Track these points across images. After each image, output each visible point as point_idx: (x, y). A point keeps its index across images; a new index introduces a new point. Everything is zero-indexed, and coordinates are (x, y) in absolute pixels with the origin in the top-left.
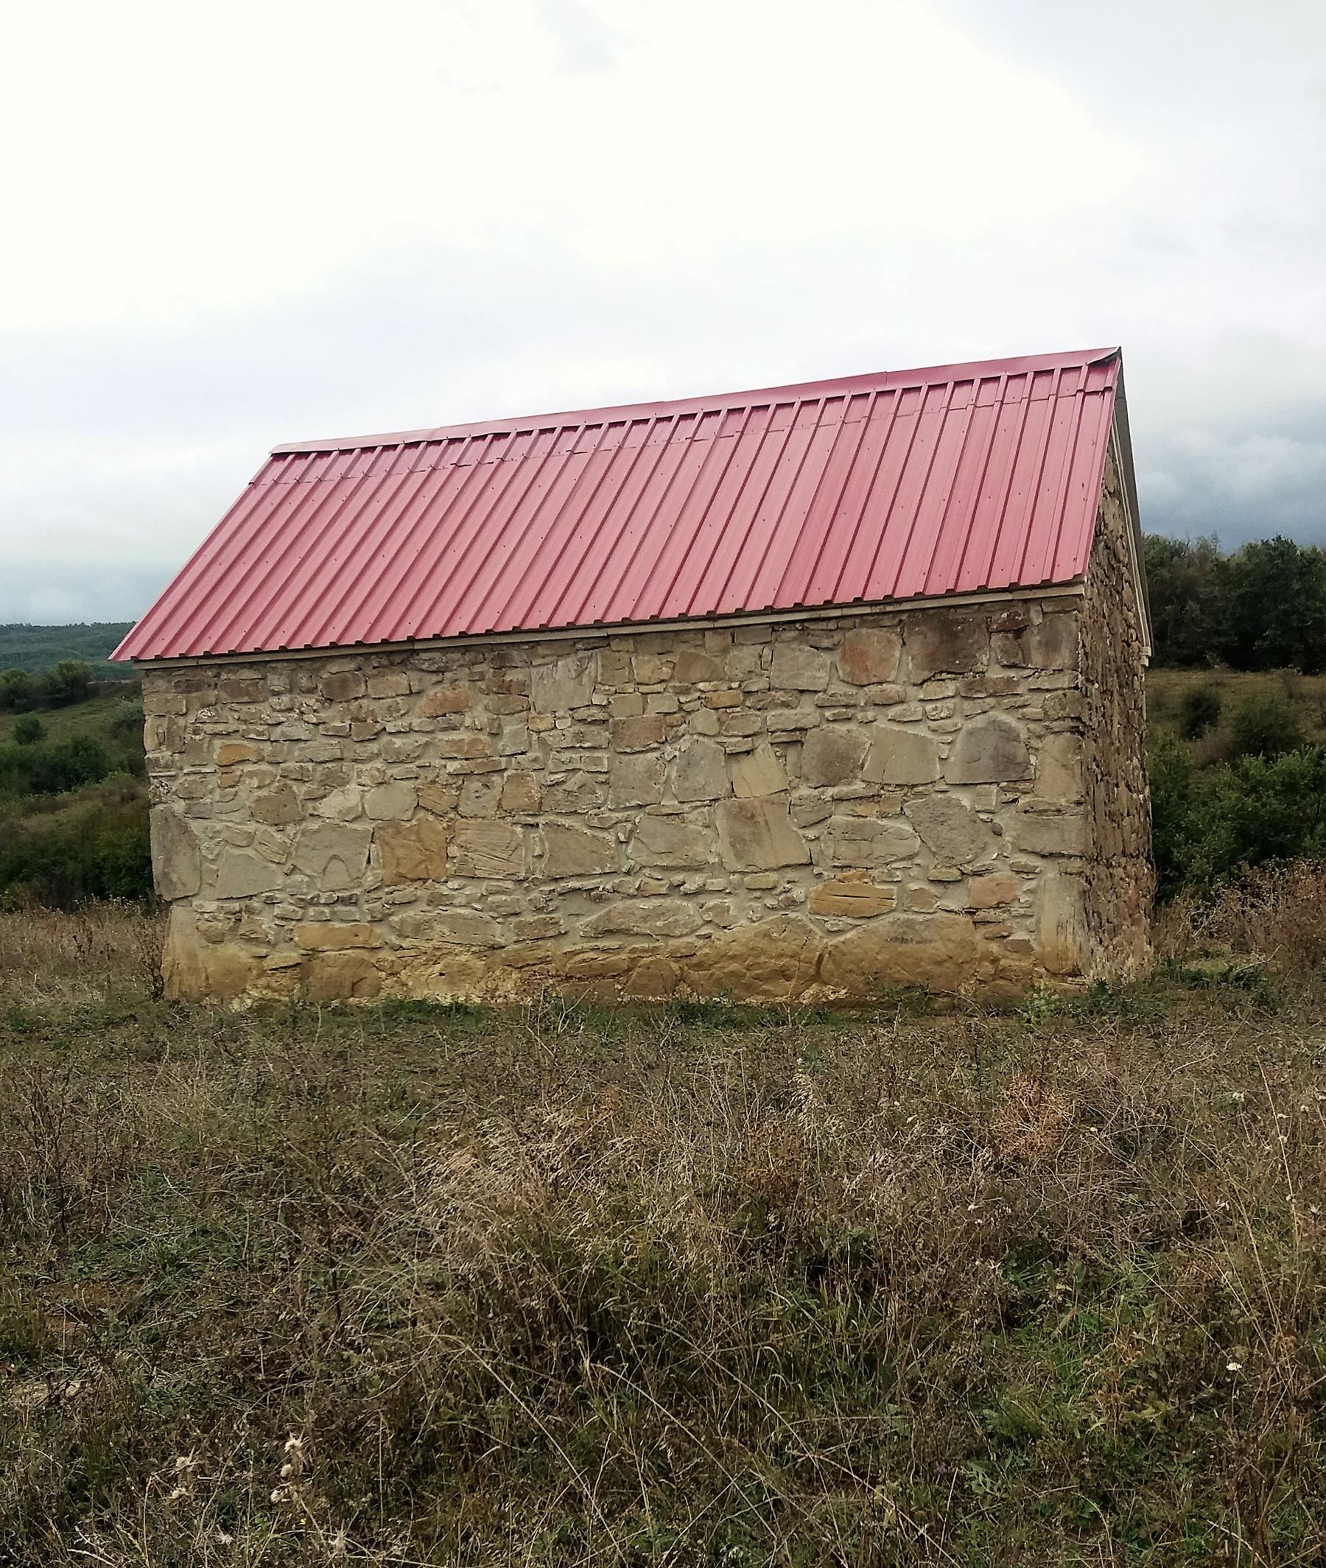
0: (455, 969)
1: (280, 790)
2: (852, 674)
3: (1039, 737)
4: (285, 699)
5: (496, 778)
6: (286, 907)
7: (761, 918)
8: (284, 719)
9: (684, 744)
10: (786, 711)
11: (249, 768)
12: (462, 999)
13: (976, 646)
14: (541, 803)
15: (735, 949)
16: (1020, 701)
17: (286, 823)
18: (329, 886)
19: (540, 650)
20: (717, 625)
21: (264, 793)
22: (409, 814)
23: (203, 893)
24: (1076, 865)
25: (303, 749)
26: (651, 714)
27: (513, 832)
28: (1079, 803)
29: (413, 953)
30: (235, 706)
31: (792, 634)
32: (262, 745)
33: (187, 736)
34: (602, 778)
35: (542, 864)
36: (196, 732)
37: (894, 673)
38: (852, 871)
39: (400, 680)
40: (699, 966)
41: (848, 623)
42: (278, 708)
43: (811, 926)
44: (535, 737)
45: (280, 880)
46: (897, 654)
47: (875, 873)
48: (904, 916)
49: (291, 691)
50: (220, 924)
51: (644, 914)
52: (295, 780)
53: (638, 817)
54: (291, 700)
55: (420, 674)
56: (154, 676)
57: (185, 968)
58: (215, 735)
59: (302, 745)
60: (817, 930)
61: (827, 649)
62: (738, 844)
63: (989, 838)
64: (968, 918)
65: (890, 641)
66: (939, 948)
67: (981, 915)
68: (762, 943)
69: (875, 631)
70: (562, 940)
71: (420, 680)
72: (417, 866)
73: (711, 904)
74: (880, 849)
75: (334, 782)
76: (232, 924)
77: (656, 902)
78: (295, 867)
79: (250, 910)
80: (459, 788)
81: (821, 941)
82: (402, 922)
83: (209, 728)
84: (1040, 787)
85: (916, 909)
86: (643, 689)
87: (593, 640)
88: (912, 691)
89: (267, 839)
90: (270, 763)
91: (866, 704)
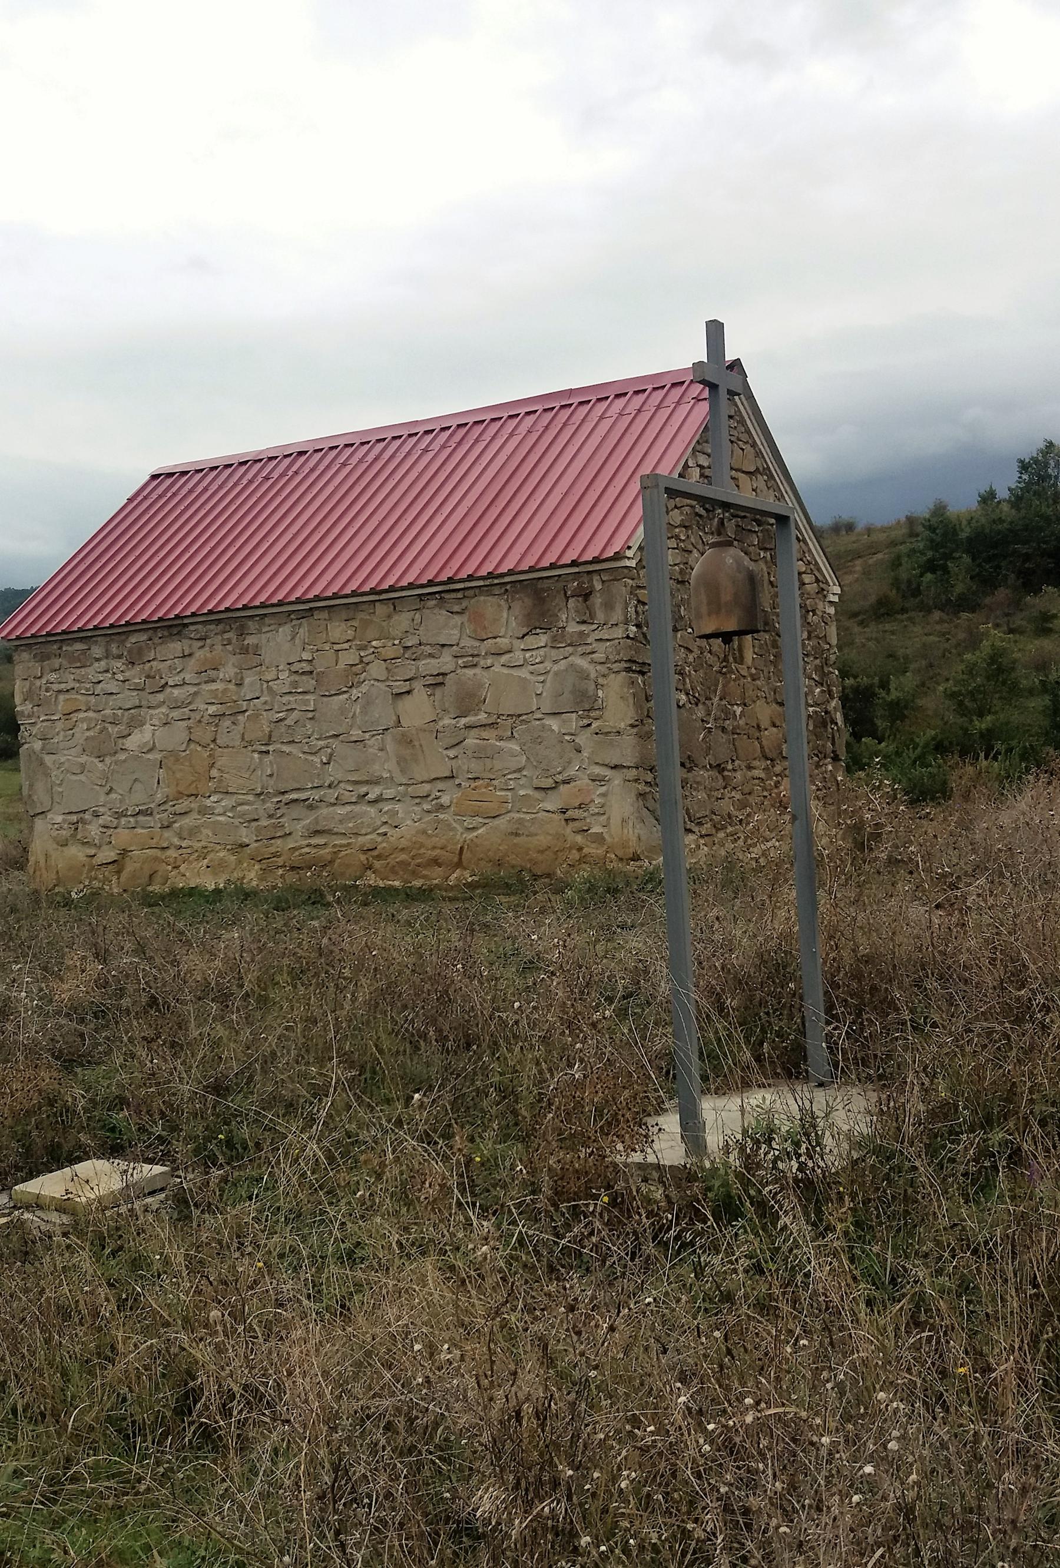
1: (101, 732)
2: (475, 631)
3: (604, 676)
4: (103, 663)
5: (240, 717)
6: (106, 819)
7: (420, 819)
9: (364, 688)
10: (432, 661)
11: (82, 715)
14: (270, 736)
15: (404, 843)
16: (589, 649)
17: (105, 755)
19: (267, 620)
21: (91, 733)
22: (184, 745)
24: (632, 773)
26: (341, 665)
27: (252, 758)
28: (632, 726)
29: (189, 851)
31: (434, 602)
34: (310, 715)
35: (271, 782)
37: (503, 630)
38: (481, 782)
39: (176, 647)
40: (379, 857)
43: (455, 825)
45: (102, 799)
46: (505, 615)
48: (517, 816)
49: (107, 658)
50: (64, 832)
53: (335, 743)
54: (107, 664)
55: (190, 642)
58: (60, 691)
60: (458, 827)
61: (457, 613)
62: (401, 761)
63: (573, 754)
64: (562, 816)
65: (499, 606)
66: (543, 840)
67: (569, 813)
68: (422, 839)
69: (489, 598)
70: (289, 839)
71: (190, 646)
73: (386, 809)
74: (498, 764)
75: (135, 724)
77: (348, 808)
78: (111, 789)
80: (217, 725)
81: (462, 837)
82: (181, 827)
83: (55, 687)
84: (607, 714)
85: (524, 810)
86: (336, 647)
88: (516, 642)
91: (486, 654)
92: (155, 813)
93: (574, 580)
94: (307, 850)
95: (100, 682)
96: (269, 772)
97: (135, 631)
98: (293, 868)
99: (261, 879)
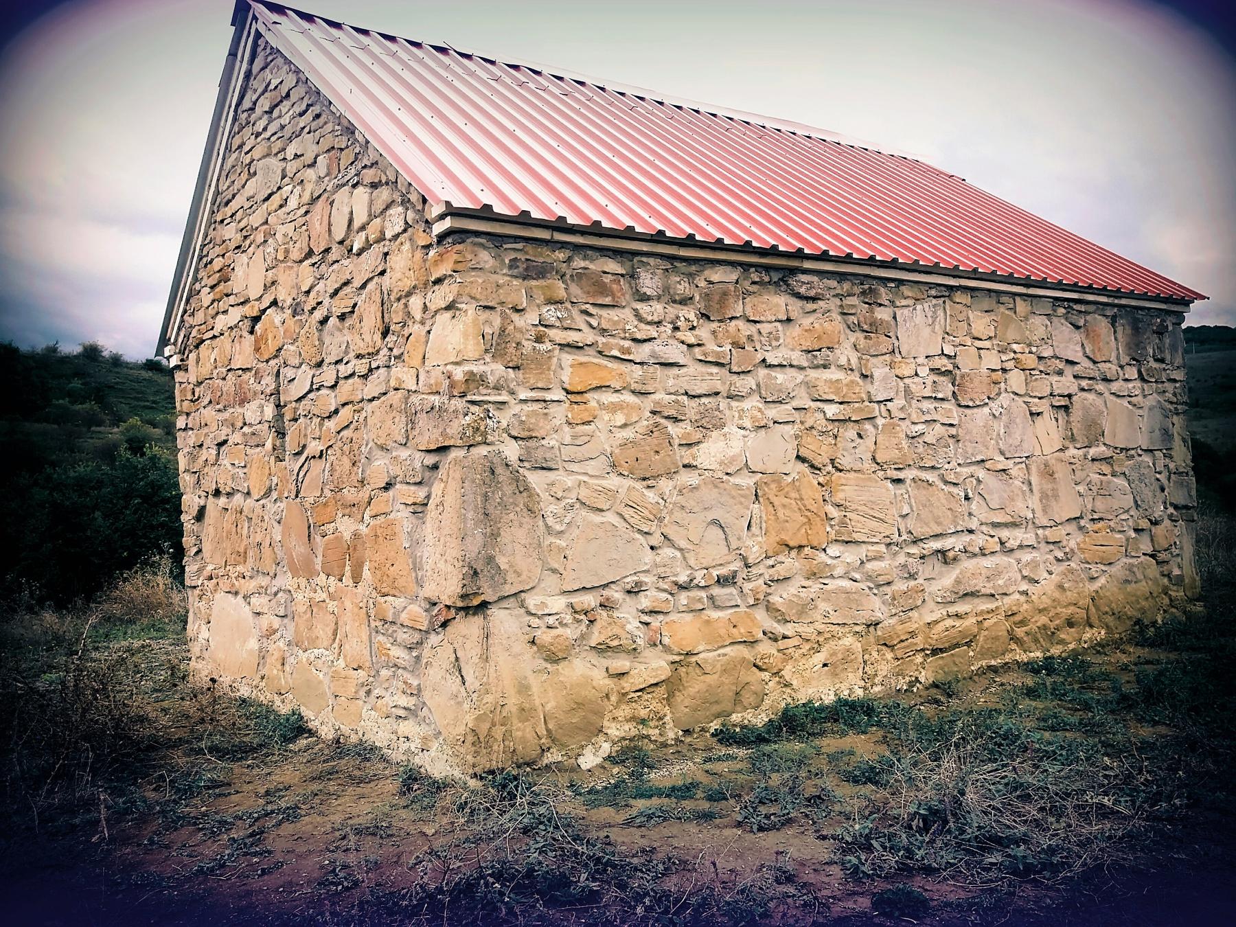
0: (840, 656)
8: (655, 334)
9: (1005, 399)
11: (608, 398)
12: (846, 693)
15: (1046, 601)
17: (656, 477)
19: (906, 290)
20: (1032, 291)
21: (628, 433)
23: (543, 585)
30: (592, 310)
33: (525, 343)
34: (953, 431)
36: (539, 339)
39: (779, 303)
40: (1022, 623)
41: (1091, 308)
42: (650, 318)
44: (901, 384)
45: (649, 556)
47: (1112, 523)
50: (568, 631)
51: (989, 574)
52: (667, 418)
56: (475, 244)
57: (514, 709)
58: (564, 346)
59: (675, 371)
62: (1044, 497)
68: (1057, 595)
75: (709, 424)
76: (583, 628)
83: (558, 335)
87: (943, 289)
92: (739, 580)
94: (949, 622)
95: (650, 340)
96: (906, 510)
98: (935, 652)
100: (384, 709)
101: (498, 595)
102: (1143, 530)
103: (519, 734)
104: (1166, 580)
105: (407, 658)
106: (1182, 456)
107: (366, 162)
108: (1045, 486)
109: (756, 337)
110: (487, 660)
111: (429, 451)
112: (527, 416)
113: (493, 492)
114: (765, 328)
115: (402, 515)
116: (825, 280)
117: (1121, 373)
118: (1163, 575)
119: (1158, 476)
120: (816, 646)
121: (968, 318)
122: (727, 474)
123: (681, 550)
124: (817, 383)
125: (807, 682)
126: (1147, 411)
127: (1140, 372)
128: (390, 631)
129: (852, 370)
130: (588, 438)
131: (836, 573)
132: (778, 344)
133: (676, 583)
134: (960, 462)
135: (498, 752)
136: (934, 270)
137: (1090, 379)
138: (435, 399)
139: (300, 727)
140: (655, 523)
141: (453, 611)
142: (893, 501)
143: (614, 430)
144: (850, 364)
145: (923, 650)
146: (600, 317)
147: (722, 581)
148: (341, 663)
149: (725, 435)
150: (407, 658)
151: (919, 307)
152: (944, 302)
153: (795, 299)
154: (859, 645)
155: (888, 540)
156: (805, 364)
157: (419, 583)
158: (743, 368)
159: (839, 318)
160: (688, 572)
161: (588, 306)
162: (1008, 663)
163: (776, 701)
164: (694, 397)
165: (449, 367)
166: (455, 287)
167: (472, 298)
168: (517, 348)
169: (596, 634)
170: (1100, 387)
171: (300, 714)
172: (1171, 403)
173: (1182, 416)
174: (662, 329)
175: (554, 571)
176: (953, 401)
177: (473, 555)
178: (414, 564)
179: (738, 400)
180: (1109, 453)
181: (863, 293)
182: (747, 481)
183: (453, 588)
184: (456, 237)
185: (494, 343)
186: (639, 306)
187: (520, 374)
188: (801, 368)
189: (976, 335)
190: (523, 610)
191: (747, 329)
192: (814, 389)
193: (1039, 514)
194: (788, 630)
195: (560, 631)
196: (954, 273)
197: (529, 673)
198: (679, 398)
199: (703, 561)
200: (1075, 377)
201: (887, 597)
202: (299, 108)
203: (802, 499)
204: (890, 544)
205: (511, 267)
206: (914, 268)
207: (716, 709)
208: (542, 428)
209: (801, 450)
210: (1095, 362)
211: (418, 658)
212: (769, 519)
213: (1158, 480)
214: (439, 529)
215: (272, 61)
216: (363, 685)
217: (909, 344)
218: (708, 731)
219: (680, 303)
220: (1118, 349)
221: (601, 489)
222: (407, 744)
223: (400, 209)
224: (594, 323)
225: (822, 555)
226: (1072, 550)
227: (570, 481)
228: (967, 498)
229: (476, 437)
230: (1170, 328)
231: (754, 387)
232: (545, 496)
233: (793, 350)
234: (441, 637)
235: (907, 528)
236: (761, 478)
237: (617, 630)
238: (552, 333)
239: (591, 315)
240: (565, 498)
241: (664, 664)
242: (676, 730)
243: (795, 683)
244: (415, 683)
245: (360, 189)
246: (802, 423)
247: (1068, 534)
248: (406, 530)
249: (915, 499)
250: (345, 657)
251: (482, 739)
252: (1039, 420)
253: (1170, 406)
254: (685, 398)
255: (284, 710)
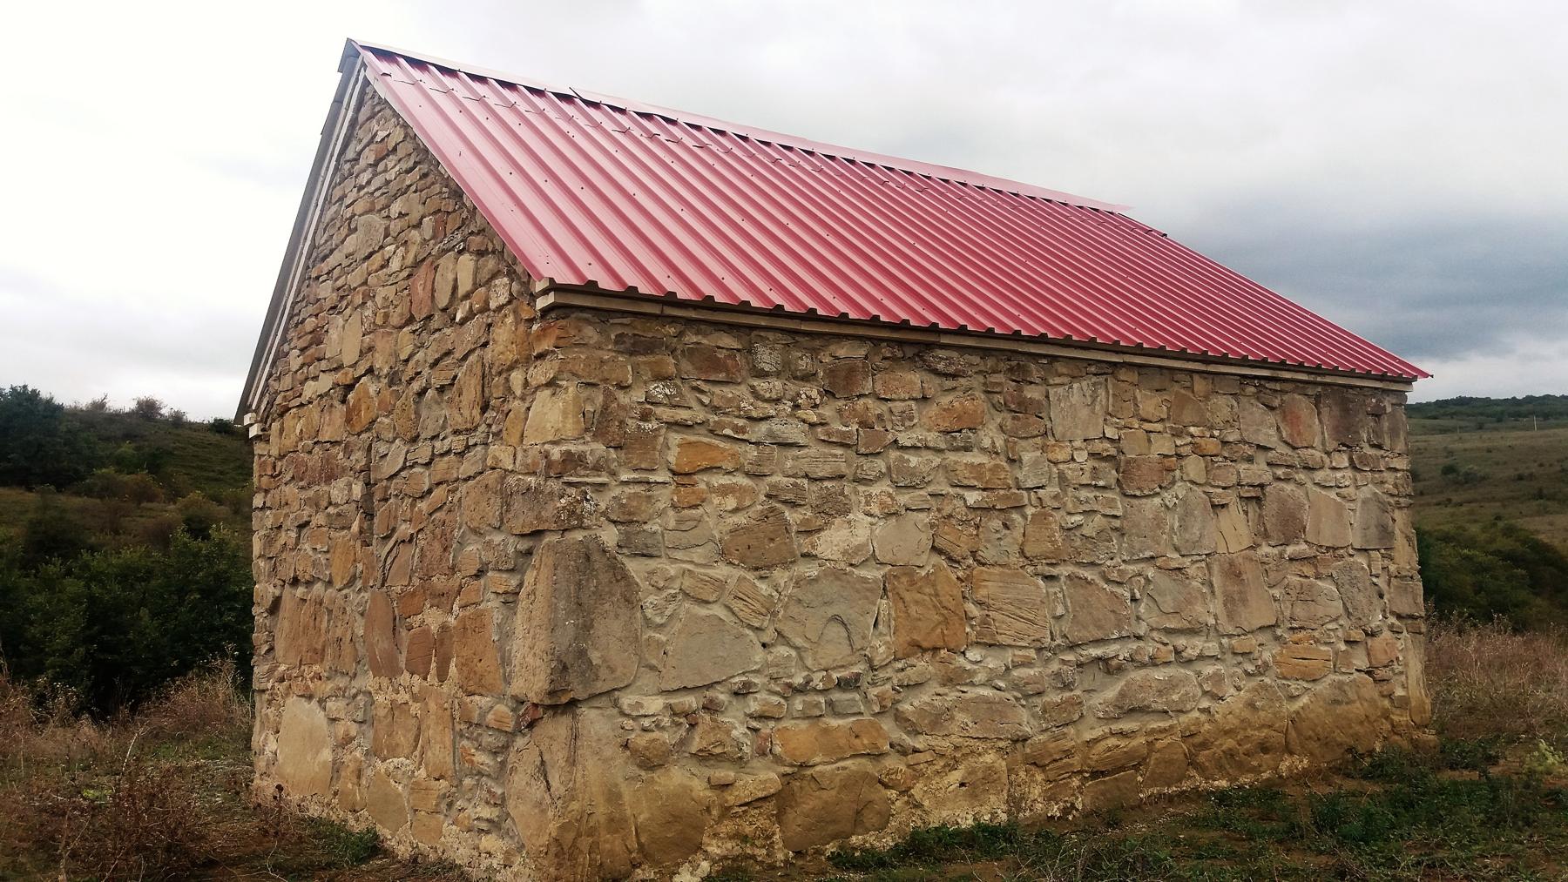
0: (980, 775)
8: (773, 412)
9: (1180, 489)
11: (719, 480)
13: (1360, 424)
15: (1233, 721)
17: (770, 567)
18: (824, 663)
20: (1211, 368)
21: (740, 519)
23: (639, 684)
25: (796, 458)
26: (1154, 456)
32: (738, 448)
33: (630, 422)
34: (1117, 523)
36: (645, 417)
39: (914, 379)
40: (1204, 745)
42: (767, 395)
45: (759, 656)
47: (1316, 634)
50: (666, 736)
52: (785, 502)
56: (579, 319)
57: (602, 819)
59: (795, 452)
62: (1229, 601)
63: (1376, 600)
66: (1358, 709)
68: (1247, 714)
72: (933, 629)
75: (833, 508)
76: (682, 732)
79: (711, 707)
80: (977, 527)
83: (665, 413)
87: (1104, 365)
89: (749, 593)
90: (747, 474)
93: (1373, 396)
94: (1112, 741)
96: (1060, 611)
97: (847, 337)
98: (1095, 774)
99: (1050, 798)
100: (466, 822)
101: (589, 692)
102: (1356, 642)
103: (608, 846)
104: (1386, 703)
105: (492, 763)
106: (1406, 557)
107: (473, 228)
108: (1230, 588)
109: (887, 416)
110: (573, 764)
111: (523, 536)
112: (629, 498)
113: (587, 580)
114: (898, 406)
115: (492, 604)
116: (966, 356)
117: (1327, 460)
118: (1383, 696)
119: (1375, 580)
120: (952, 762)
121: (1135, 398)
122: (851, 565)
123: (797, 648)
124: (957, 467)
125: (940, 803)
126: (1359, 504)
127: (1351, 460)
128: (475, 734)
129: (997, 453)
130: (694, 523)
131: (976, 680)
132: (912, 424)
133: (789, 685)
134: (1125, 558)
135: (584, 865)
136: (1090, 345)
137: (1288, 467)
138: (531, 480)
139: (375, 846)
140: (768, 618)
141: (541, 710)
142: (1045, 601)
143: (724, 515)
144: (994, 447)
145: (1080, 772)
146: (713, 394)
147: (843, 685)
148: (422, 773)
149: (849, 522)
150: (492, 763)
151: (1075, 386)
152: (1106, 380)
153: (933, 376)
154: (1004, 763)
155: (1039, 645)
156: (943, 446)
157: (507, 680)
158: (871, 449)
159: (983, 396)
160: (806, 673)
161: (699, 382)
162: (1185, 791)
163: (904, 820)
164: (816, 480)
165: (546, 446)
166: (556, 364)
167: (574, 374)
168: (620, 427)
169: (697, 739)
170: (1301, 476)
171: (375, 833)
172: (1392, 495)
173: (1405, 510)
174: (781, 407)
175: (652, 668)
176: (1118, 489)
177: (563, 648)
178: (503, 658)
179: (864, 485)
180: (1310, 552)
181: (1011, 370)
182: (872, 574)
183: (540, 684)
184: (560, 312)
185: (595, 421)
186: (756, 382)
187: (622, 454)
188: (939, 451)
189: (1144, 415)
190: (615, 711)
191: (876, 408)
192: (953, 474)
193: (1223, 620)
194: (919, 742)
195: (656, 734)
196: (1115, 348)
197: (620, 780)
198: (798, 481)
199: (822, 661)
200: (1268, 464)
201: (1038, 709)
202: (405, 166)
203: (937, 595)
204: (1041, 649)
205: (616, 343)
206: (1067, 343)
207: (831, 829)
208: (644, 511)
209: (937, 541)
210: (1294, 448)
211: (503, 763)
212: (898, 617)
213: (1376, 585)
214: (530, 619)
215: (379, 112)
216: (444, 796)
217: (1064, 427)
218: (823, 854)
219: (802, 380)
220: (1323, 433)
221: (707, 579)
222: (489, 861)
223: (506, 279)
224: (706, 400)
225: (961, 659)
226: (1266, 664)
227: (672, 570)
228: (1134, 599)
229: (573, 519)
230: (1389, 409)
231: (884, 470)
232: (644, 585)
233: (929, 430)
234: (526, 739)
235: (1061, 631)
236: (890, 571)
237: (720, 736)
238: (659, 410)
239: (702, 392)
240: (667, 588)
241: (774, 776)
242: (786, 851)
243: (926, 803)
244: (499, 791)
245: (466, 257)
246: (939, 510)
247: (1260, 645)
248: (495, 621)
249: (1071, 599)
250: (427, 765)
251: (566, 849)
252: (1223, 513)
253: (1392, 500)
254: (806, 481)
255: (356, 826)
